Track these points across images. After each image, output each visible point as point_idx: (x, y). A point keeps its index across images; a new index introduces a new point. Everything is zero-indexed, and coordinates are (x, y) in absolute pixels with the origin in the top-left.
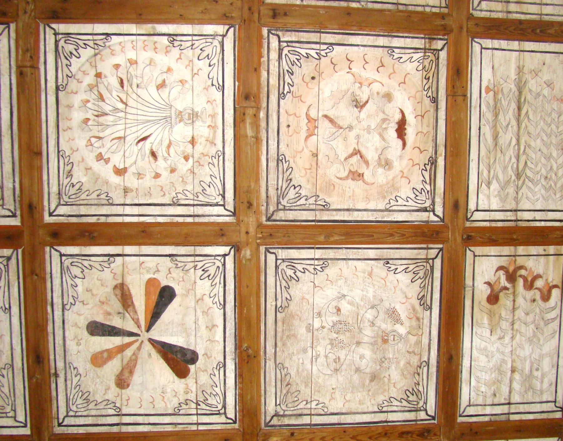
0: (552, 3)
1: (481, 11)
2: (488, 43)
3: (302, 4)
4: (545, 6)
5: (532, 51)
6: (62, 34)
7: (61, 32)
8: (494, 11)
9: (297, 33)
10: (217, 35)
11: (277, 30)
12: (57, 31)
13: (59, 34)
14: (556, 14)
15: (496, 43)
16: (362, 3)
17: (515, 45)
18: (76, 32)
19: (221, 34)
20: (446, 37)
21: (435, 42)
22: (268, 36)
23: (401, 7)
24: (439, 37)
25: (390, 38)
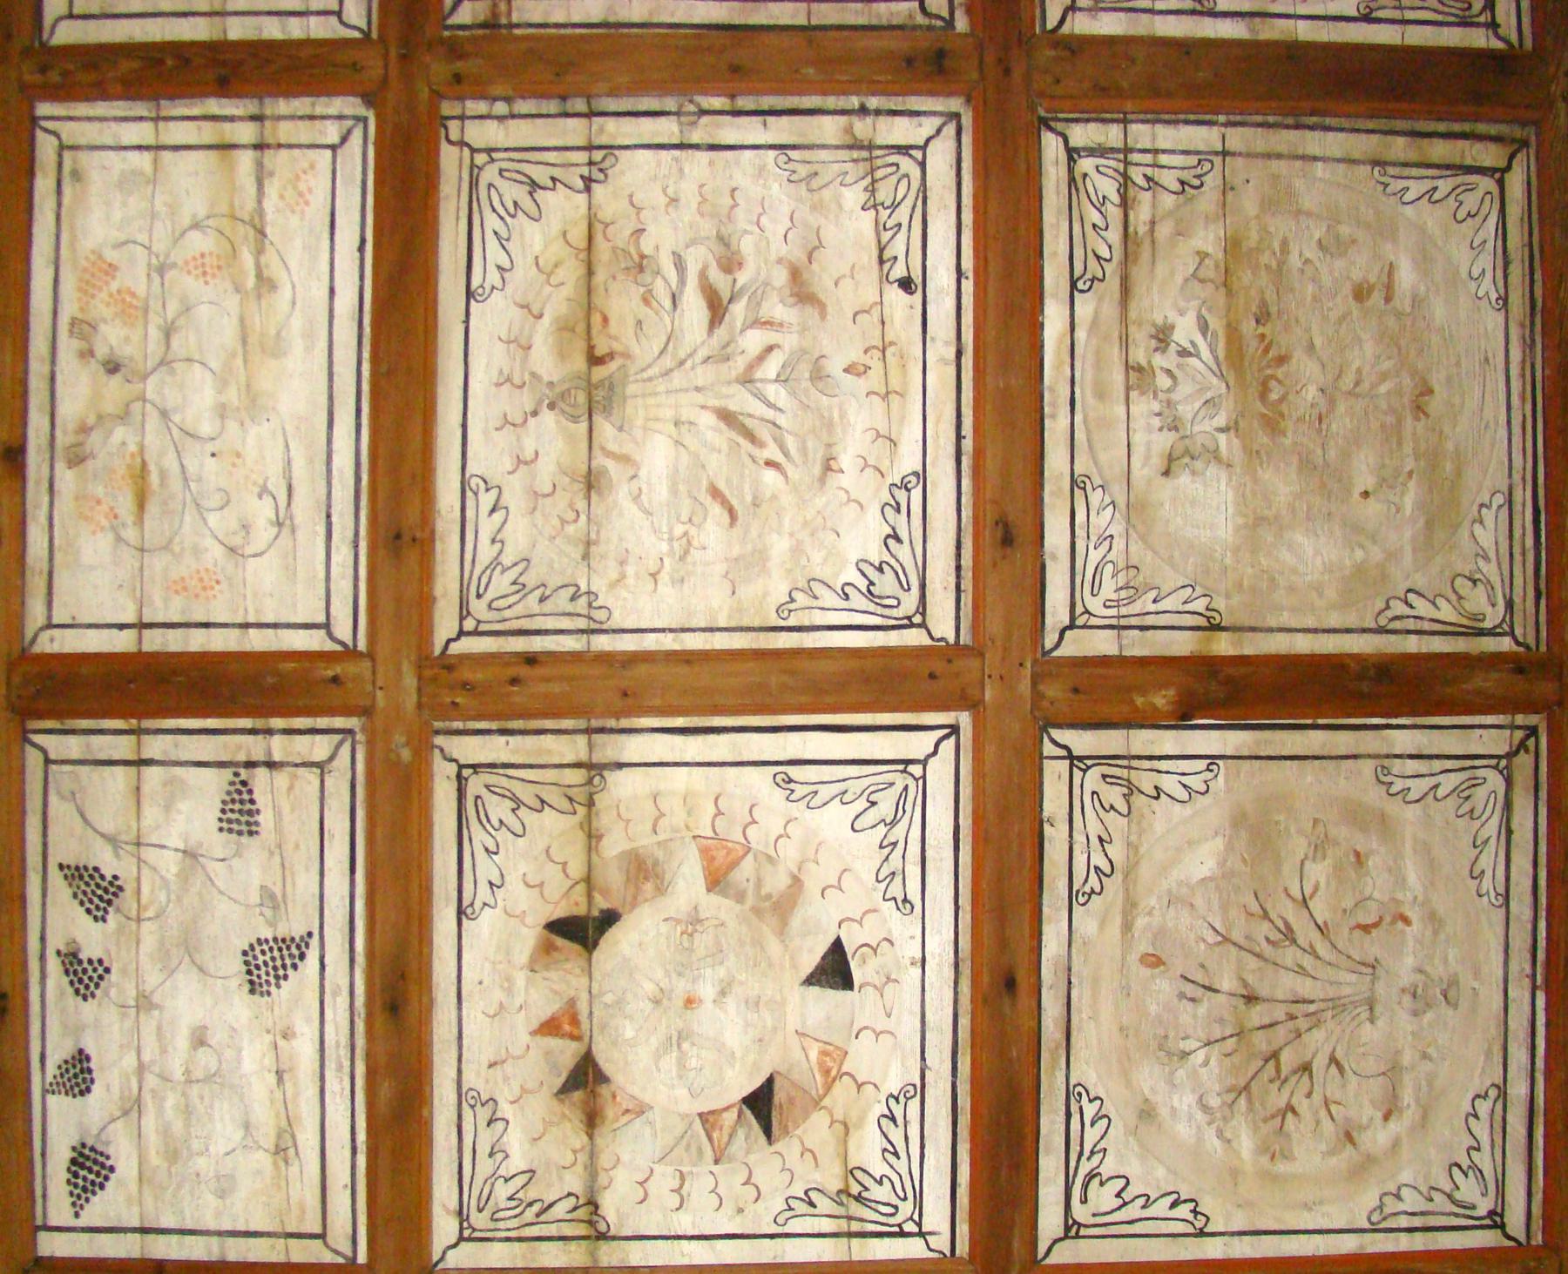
0: (123, 153)
1: (340, 117)
2: (319, 29)
3: (864, 99)
4: (144, 143)
5: (185, 15)
6: (1478, 25)
7: (1482, 31)
8: (301, 118)
9: (874, 22)
10: (1089, 10)
11: (930, 28)
12: (1490, 32)
13: (1486, 25)
14: (113, 124)
15: (295, 29)
16: (692, 108)
17: (237, 30)
18: (1445, 29)
19: (1078, 14)
20: (447, 33)
21: (481, 18)
22: (952, 13)
23: (580, 105)
24: (467, 33)
25: (612, 19)
